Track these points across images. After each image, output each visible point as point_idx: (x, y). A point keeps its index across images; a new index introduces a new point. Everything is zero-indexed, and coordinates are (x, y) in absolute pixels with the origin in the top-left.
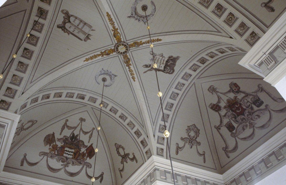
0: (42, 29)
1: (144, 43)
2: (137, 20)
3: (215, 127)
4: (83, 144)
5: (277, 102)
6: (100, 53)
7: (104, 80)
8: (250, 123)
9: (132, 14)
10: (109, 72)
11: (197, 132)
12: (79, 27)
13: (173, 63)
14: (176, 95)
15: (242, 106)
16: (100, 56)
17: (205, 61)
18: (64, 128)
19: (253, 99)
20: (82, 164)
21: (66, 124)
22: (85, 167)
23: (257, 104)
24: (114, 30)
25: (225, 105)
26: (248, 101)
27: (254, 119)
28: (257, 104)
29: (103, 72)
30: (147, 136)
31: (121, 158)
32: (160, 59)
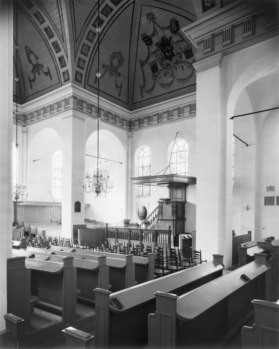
3: (140, 60)
11: (120, 62)
14: (109, 10)
15: (173, 50)
25: (158, 41)
31: (32, 67)
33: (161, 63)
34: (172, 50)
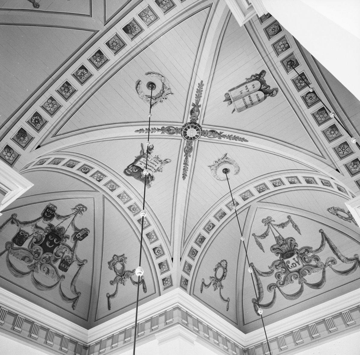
0: (275, 49)
1: (186, 158)
2: (217, 161)
5: (71, 286)
6: (199, 104)
7: (152, 85)
8: (35, 264)
9: (227, 158)
10: (163, 100)
12: (248, 96)
13: (142, 177)
15: (57, 247)
16: (196, 103)
17: (134, 211)
19: (67, 258)
23: (62, 265)
24: (221, 135)
25: (55, 226)
26: (64, 253)
27: (42, 267)
28: (62, 265)
29: (166, 91)
30: (39, 147)
32: (154, 166)
33: (32, 243)
34: (56, 245)
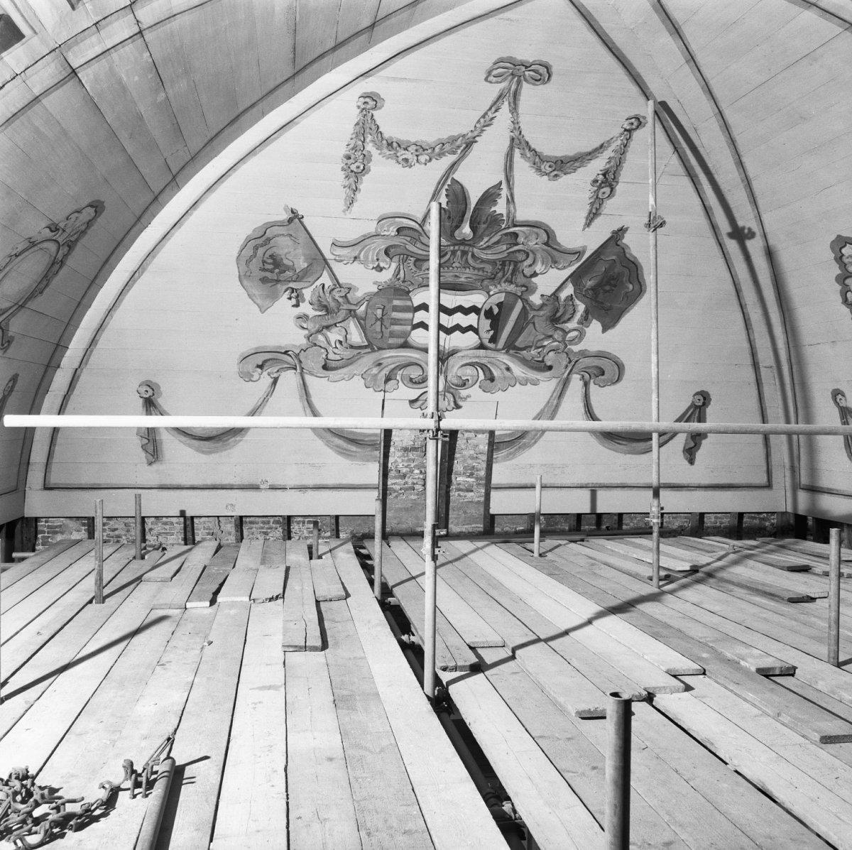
4: (546, 244)
18: (367, 158)
20: (550, 368)
21: (366, 127)
22: (576, 383)
